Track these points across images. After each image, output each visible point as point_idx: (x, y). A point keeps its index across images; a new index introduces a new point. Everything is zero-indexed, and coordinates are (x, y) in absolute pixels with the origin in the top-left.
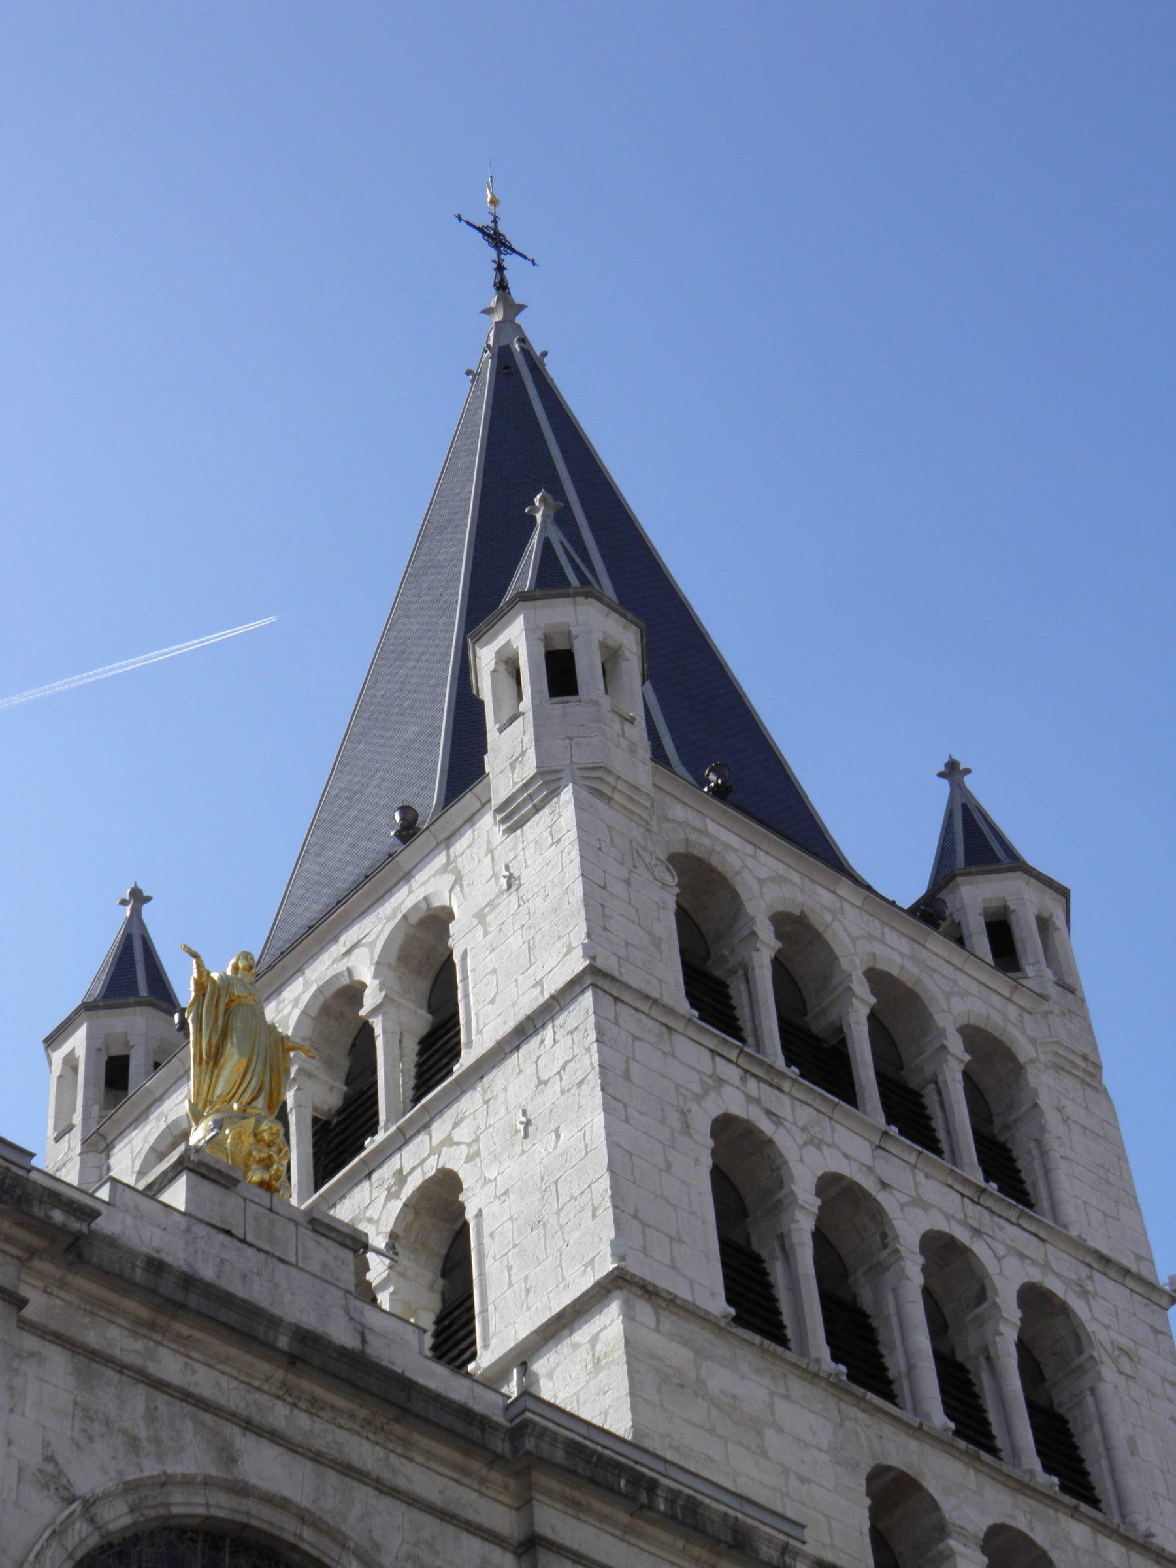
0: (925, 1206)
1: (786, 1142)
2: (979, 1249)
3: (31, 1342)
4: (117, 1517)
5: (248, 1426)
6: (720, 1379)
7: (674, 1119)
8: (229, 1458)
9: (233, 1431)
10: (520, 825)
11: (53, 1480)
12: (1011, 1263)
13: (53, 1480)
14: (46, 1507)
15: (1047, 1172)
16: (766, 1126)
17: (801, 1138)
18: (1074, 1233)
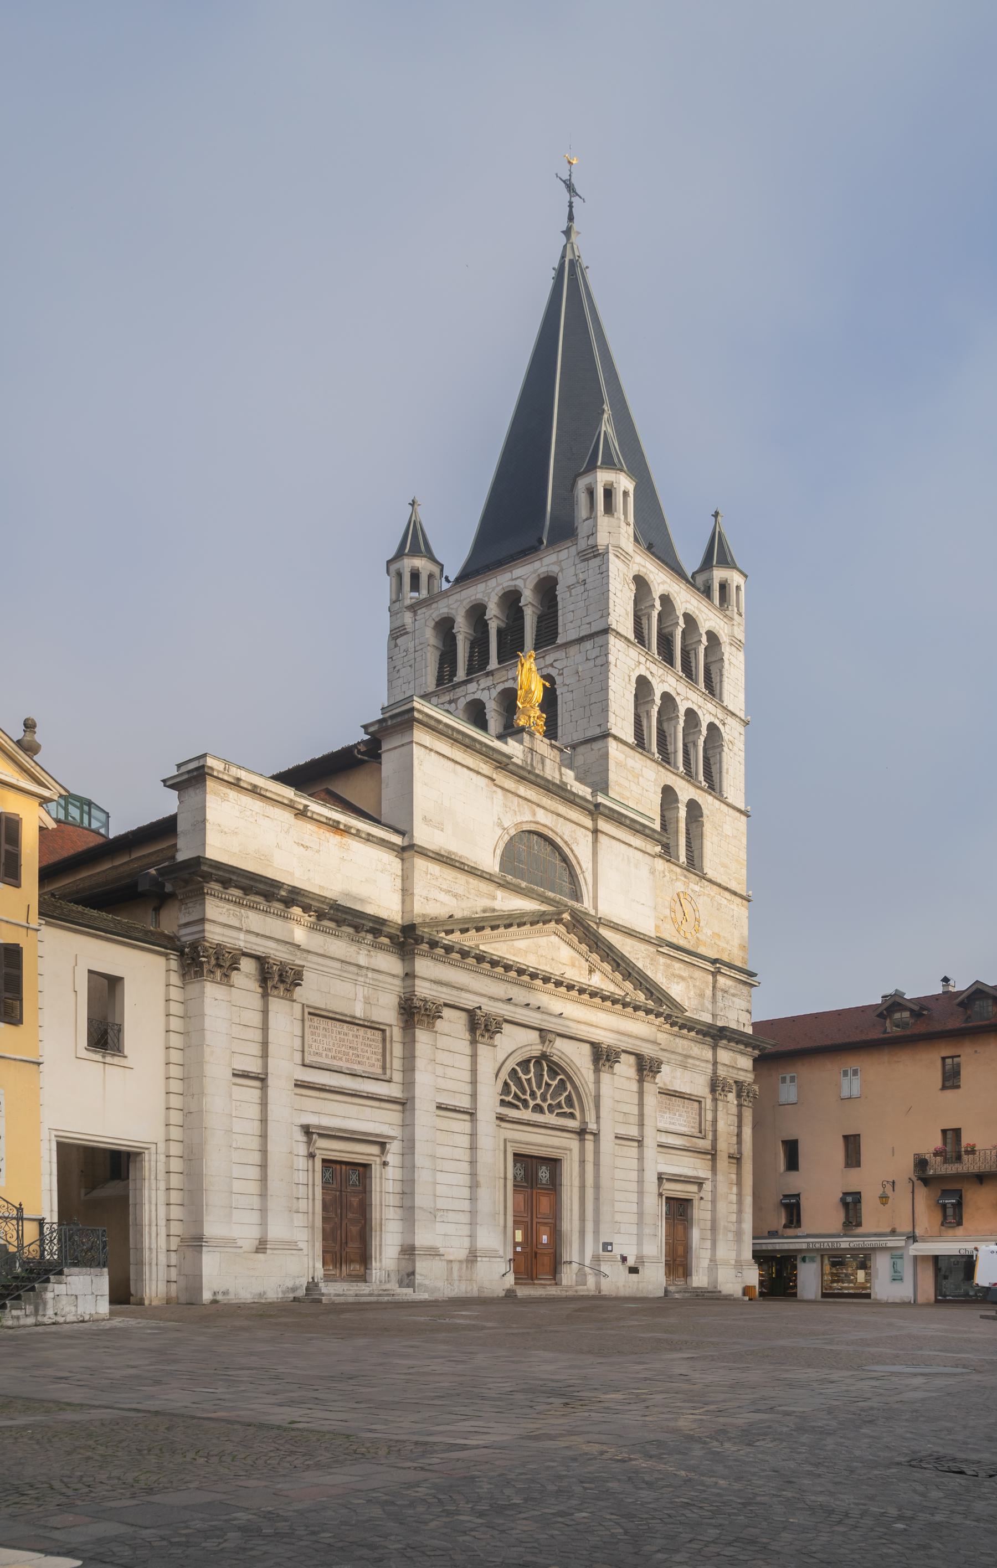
0: (688, 699)
1: (654, 682)
2: (700, 713)
3: (495, 788)
4: (513, 832)
5: (538, 805)
6: (630, 762)
7: (627, 678)
8: (534, 814)
9: (534, 806)
10: (587, 560)
11: (500, 824)
12: (707, 715)
13: (500, 824)
14: (499, 832)
15: (721, 682)
16: (650, 677)
17: (658, 680)
18: (725, 704)
